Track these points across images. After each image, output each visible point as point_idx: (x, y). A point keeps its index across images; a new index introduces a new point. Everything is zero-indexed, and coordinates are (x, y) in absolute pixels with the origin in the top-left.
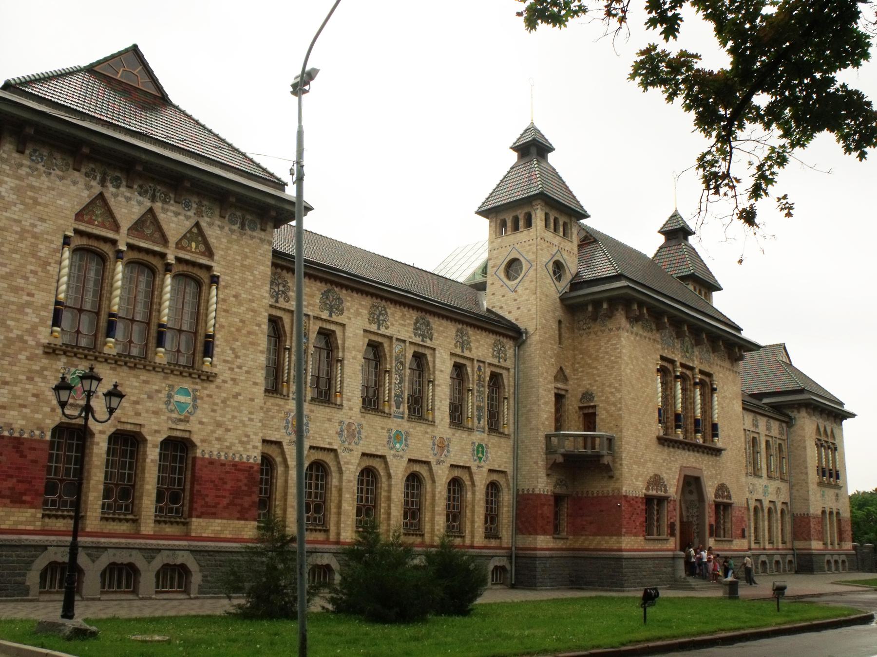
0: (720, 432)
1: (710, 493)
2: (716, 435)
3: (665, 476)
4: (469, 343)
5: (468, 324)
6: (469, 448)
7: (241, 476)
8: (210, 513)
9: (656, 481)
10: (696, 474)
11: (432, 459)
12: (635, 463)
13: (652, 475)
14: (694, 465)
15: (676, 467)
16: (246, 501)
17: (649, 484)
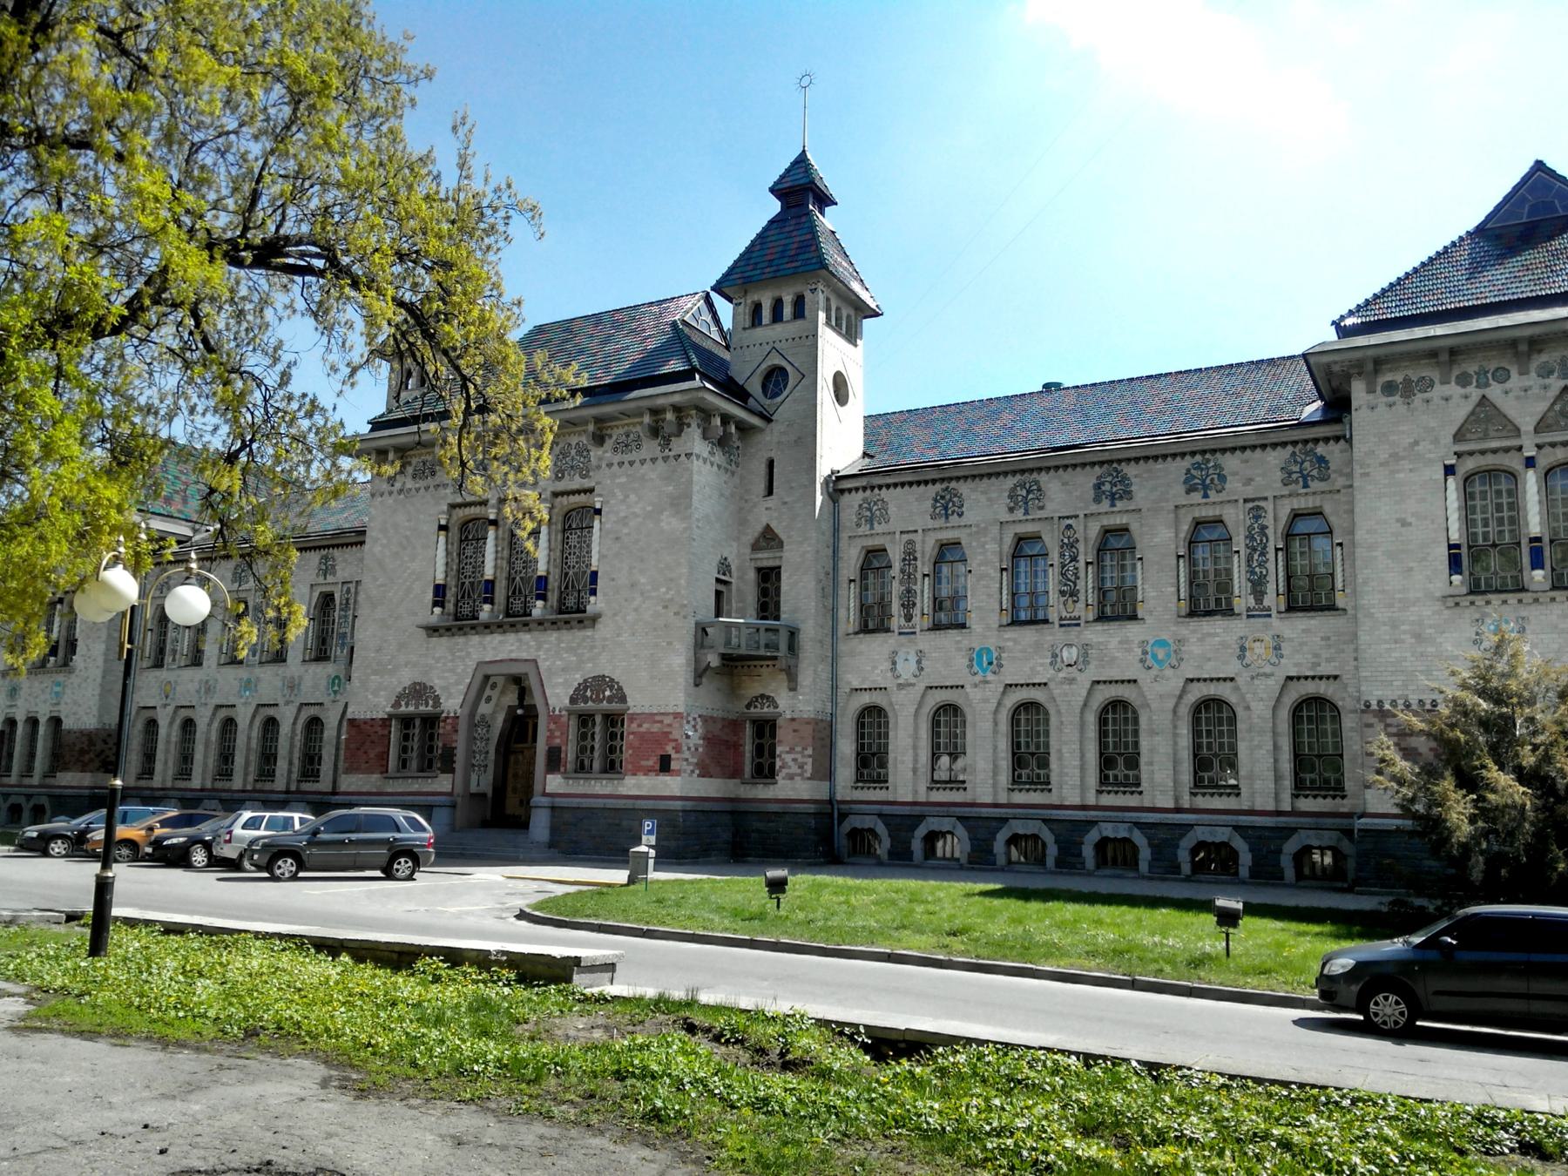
0: (601, 583)
1: (557, 694)
2: (594, 592)
3: (437, 683)
4: (333, 566)
5: (328, 547)
6: (324, 683)
7: (84, 739)
8: (65, 769)
9: (419, 691)
10: (516, 669)
11: (281, 701)
12: (375, 673)
13: (407, 683)
14: (513, 656)
15: (472, 664)
16: (87, 758)
17: (399, 697)
